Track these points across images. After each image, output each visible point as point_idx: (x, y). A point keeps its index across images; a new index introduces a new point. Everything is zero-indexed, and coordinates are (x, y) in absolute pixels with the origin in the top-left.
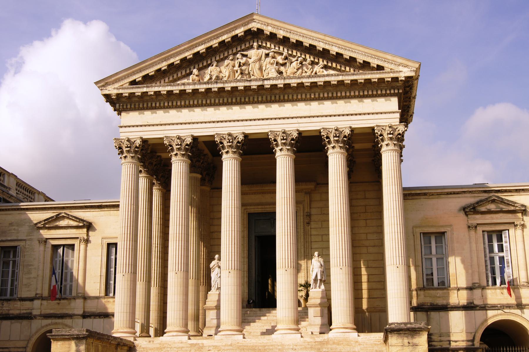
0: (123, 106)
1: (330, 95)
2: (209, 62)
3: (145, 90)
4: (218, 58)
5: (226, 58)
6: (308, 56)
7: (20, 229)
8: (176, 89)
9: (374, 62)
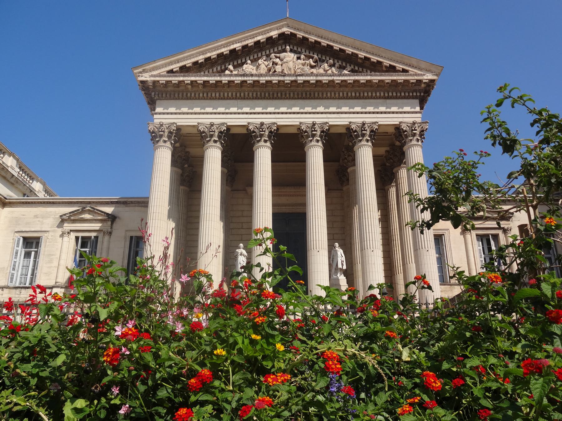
0: (158, 94)
1: (358, 95)
2: (243, 61)
3: (181, 79)
4: (252, 58)
5: (259, 58)
6: (336, 61)
7: (44, 221)
8: (212, 79)
9: (400, 67)
